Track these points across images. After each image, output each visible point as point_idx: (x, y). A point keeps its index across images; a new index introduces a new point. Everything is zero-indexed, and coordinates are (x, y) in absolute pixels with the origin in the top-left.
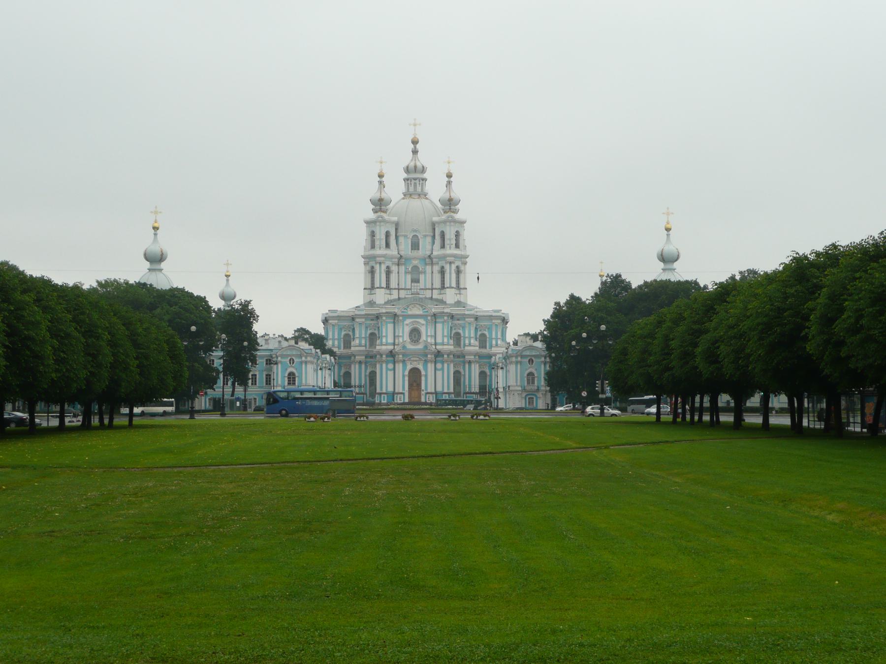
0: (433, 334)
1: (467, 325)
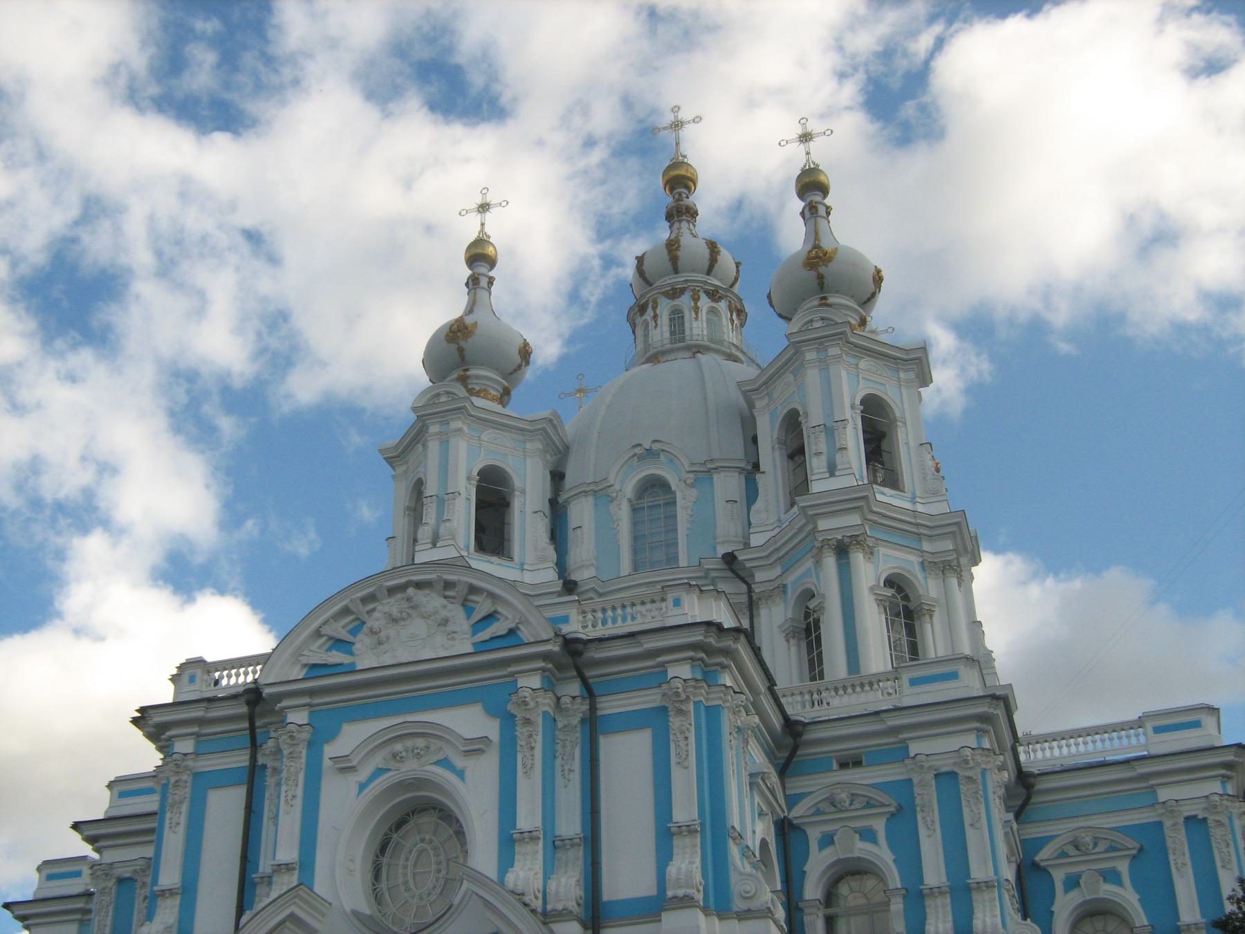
0: (570, 824)
1: (928, 795)
